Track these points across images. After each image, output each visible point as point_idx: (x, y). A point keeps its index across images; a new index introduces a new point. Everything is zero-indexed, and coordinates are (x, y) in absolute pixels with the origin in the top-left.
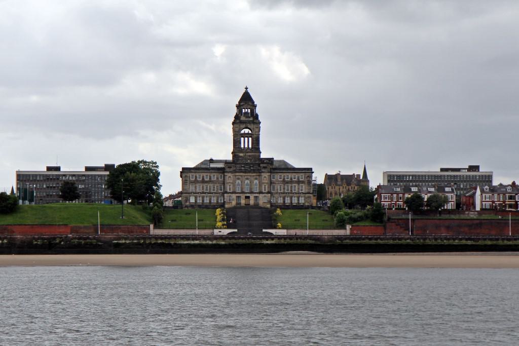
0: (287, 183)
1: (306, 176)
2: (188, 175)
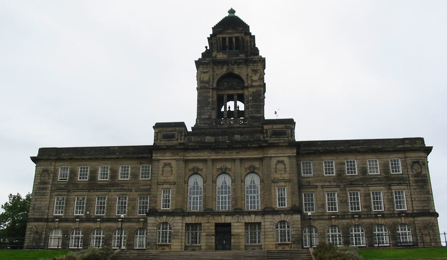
0: (352, 183)
1: (409, 161)
2: (52, 168)
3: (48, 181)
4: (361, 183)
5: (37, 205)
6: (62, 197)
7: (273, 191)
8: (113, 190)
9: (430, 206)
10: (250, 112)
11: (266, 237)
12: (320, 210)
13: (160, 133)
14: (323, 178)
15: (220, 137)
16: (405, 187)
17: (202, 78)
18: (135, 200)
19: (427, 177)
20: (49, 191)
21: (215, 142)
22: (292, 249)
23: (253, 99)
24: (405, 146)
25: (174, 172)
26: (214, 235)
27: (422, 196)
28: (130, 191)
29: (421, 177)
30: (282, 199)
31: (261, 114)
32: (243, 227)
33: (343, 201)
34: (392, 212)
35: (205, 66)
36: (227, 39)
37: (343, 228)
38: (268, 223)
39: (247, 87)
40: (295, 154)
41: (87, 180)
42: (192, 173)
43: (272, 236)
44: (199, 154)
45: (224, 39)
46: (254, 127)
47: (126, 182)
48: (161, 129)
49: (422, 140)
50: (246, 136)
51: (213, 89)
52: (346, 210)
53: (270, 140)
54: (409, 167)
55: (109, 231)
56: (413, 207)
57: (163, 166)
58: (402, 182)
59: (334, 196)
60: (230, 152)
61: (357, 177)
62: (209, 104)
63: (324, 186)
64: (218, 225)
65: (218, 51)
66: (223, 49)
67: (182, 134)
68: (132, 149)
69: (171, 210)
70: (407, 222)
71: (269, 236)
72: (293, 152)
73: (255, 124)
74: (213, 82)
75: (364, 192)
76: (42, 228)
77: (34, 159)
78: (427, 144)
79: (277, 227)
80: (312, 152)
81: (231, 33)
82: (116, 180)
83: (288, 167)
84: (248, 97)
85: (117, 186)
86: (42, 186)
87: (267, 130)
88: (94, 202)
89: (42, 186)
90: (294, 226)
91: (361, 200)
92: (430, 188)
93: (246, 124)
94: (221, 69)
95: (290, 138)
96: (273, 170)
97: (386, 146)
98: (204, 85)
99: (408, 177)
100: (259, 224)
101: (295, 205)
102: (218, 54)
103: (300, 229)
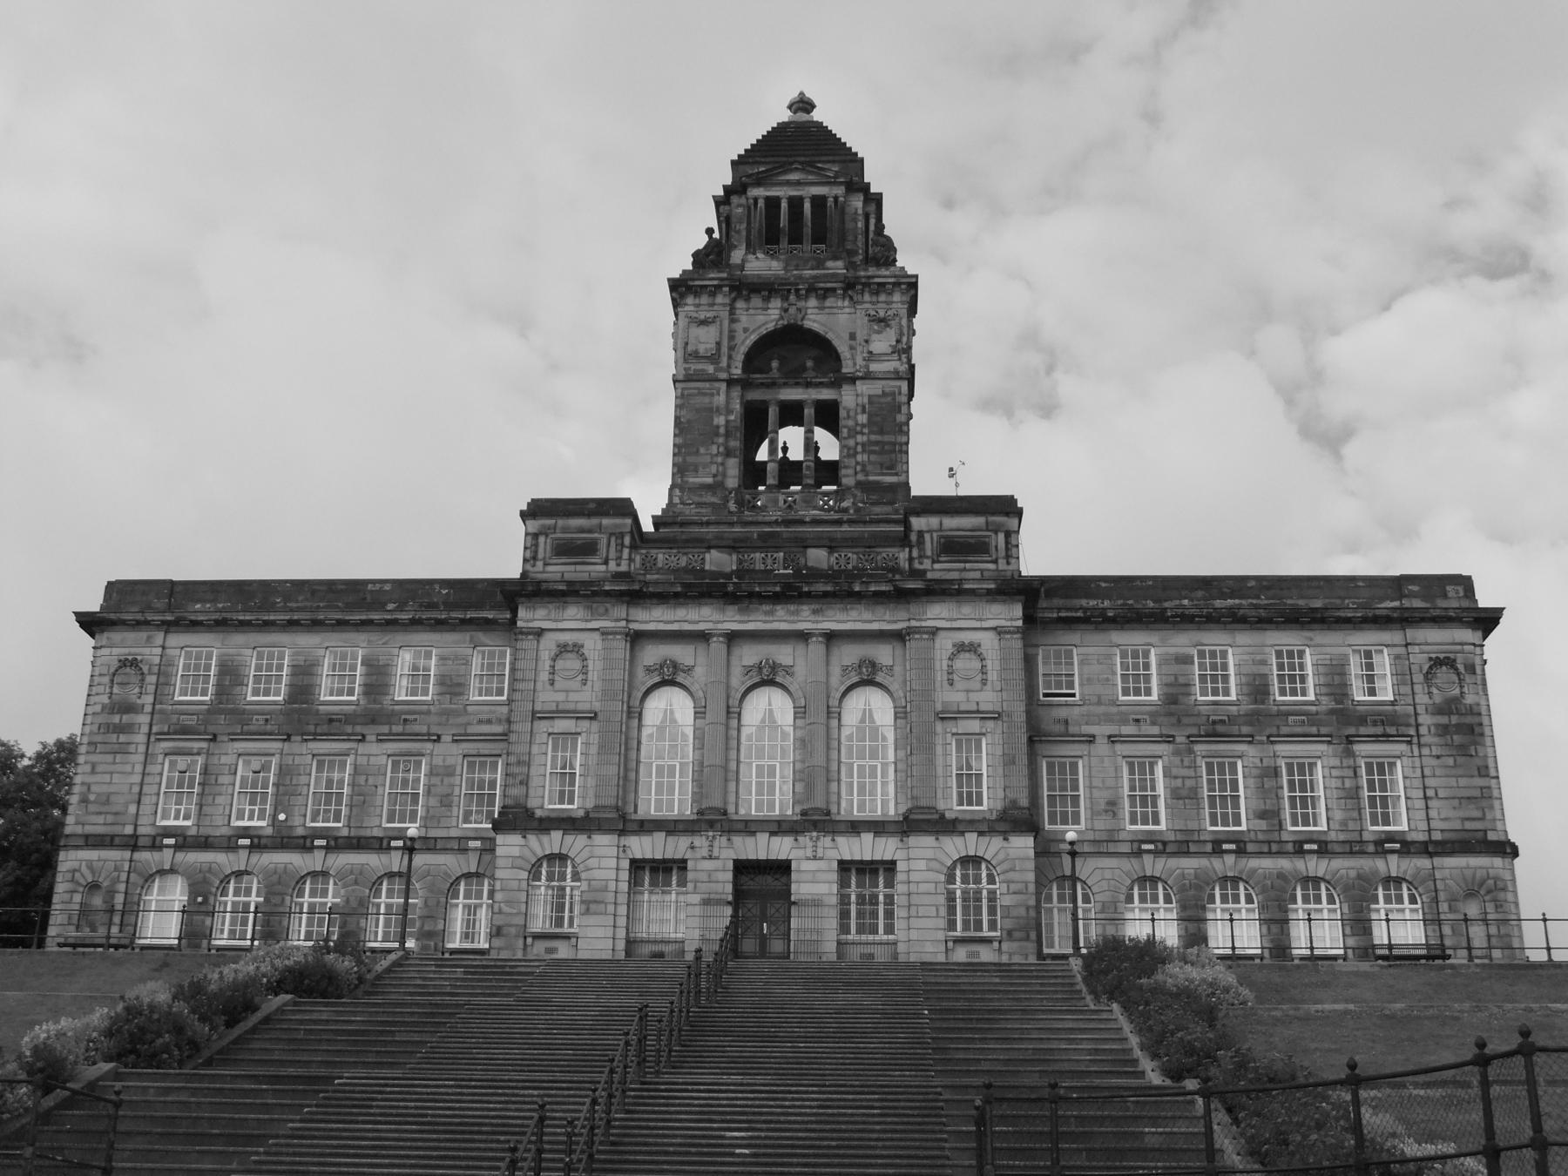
0: (1217, 730)
1: (1419, 658)
2: (151, 654)
3: (139, 701)
4: (1245, 730)
5: (93, 788)
6: (189, 758)
7: (939, 750)
8: (373, 738)
9: (1489, 816)
10: (859, 468)
11: (913, 911)
13: (547, 536)
14: (1114, 710)
15: (758, 555)
16: (1403, 747)
17: (692, 340)
18: (449, 772)
19: (1480, 714)
20: (141, 738)
21: (740, 573)
22: (1005, 959)
23: (870, 423)
24: (1406, 603)
25: (593, 675)
26: (729, 903)
27: (1463, 782)
28: (435, 741)
29: (1459, 713)
30: (968, 778)
31: (896, 474)
32: (835, 876)
33: (1184, 793)
34: (1355, 837)
35: (705, 299)
36: (784, 205)
37: (1182, 889)
38: (922, 865)
39: (852, 380)
40: (1020, 623)
41: (281, 698)
42: (657, 679)
43: (934, 908)
44: (681, 613)
45: (773, 203)
46: (872, 522)
48: (550, 522)
49: (1465, 583)
50: (850, 555)
51: (730, 382)
52: (1193, 825)
53: (933, 570)
54: (1418, 678)
55: (356, 883)
57: (553, 654)
58: (1391, 730)
59: (1152, 773)
60: (792, 608)
61: (1235, 708)
62: (717, 435)
63: (1115, 736)
64: (743, 868)
65: (751, 249)
66: (769, 238)
67: (622, 538)
68: (444, 592)
69: (581, 813)
70: (1405, 872)
71: (922, 911)
72: (1011, 614)
73: (877, 509)
74: (730, 357)
75: (1257, 761)
76: (116, 869)
77: (90, 623)
78: (1485, 599)
79: (951, 879)
80: (1080, 614)
81: (798, 183)
82: (387, 700)
83: (993, 665)
84: (852, 414)
85: (390, 724)
86: (116, 719)
87: (921, 534)
88: (303, 779)
89: (116, 719)
90: (1011, 875)
91: (1249, 791)
92: (1490, 754)
93: (845, 510)
94: (759, 311)
95: (1002, 565)
96: (941, 677)
97: (1338, 601)
98: (700, 366)
99: (1413, 713)
100: (890, 866)
101: (1014, 804)
102: (751, 257)
103: (1032, 888)
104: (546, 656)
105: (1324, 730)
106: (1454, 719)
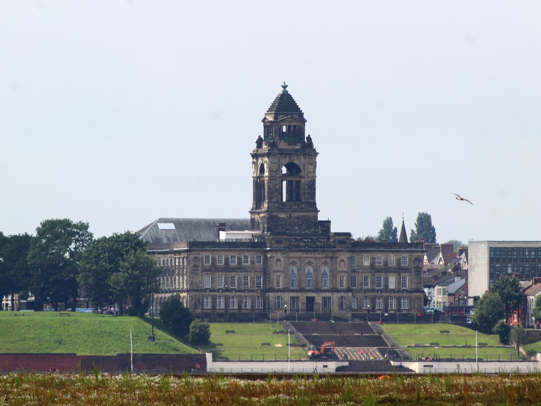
0: (379, 271)
1: (413, 258)
2: (200, 256)
4: (383, 271)
12: (360, 287)
20: (200, 272)
25: (283, 265)
27: (417, 280)
30: (341, 283)
44: (296, 254)
47: (247, 267)
52: (374, 287)
54: (412, 262)
56: (411, 287)
58: (407, 271)
64: (307, 298)
79: (339, 300)
86: (195, 268)
89: (195, 268)
96: (338, 265)
104: (275, 261)
105: (396, 271)
106: (417, 269)
